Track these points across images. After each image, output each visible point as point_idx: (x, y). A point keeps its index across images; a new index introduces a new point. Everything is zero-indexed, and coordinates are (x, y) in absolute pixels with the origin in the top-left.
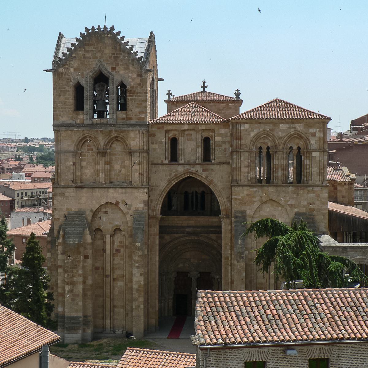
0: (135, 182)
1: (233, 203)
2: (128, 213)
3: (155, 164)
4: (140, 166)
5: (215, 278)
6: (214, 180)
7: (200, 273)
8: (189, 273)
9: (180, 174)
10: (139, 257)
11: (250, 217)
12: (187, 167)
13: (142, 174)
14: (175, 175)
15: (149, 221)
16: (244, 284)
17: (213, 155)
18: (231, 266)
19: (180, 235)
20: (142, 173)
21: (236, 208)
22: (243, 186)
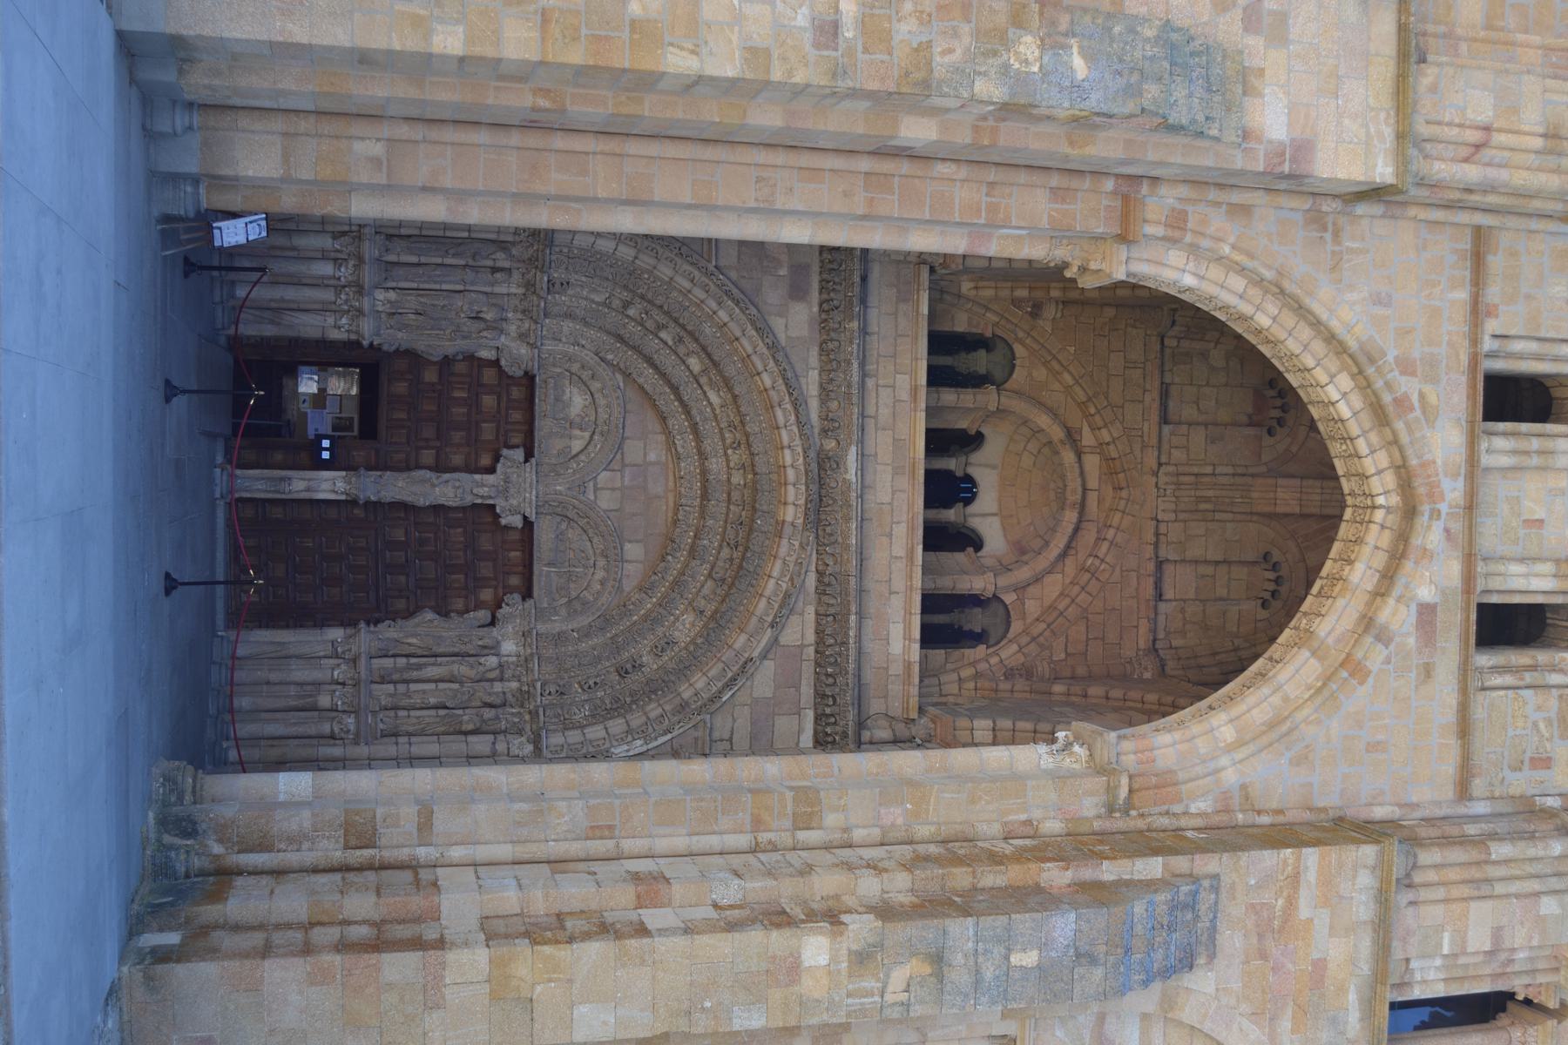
0: (1434, 89)
1: (1268, 858)
2: (1225, 10)
3: (1478, 260)
4: (1538, 143)
5: (492, 623)
6: (1363, 691)
7: (528, 523)
8: (529, 455)
9: (1404, 438)
10: (916, 50)
11: (1168, 1003)
12: (1453, 491)
13: (1478, 147)
14: (1402, 403)
15: (1109, 185)
16: (660, 1028)
17: (1508, 679)
18: (754, 850)
19: (814, 404)
20: (1487, 154)
21: (1233, 886)
22: (1383, 927)
